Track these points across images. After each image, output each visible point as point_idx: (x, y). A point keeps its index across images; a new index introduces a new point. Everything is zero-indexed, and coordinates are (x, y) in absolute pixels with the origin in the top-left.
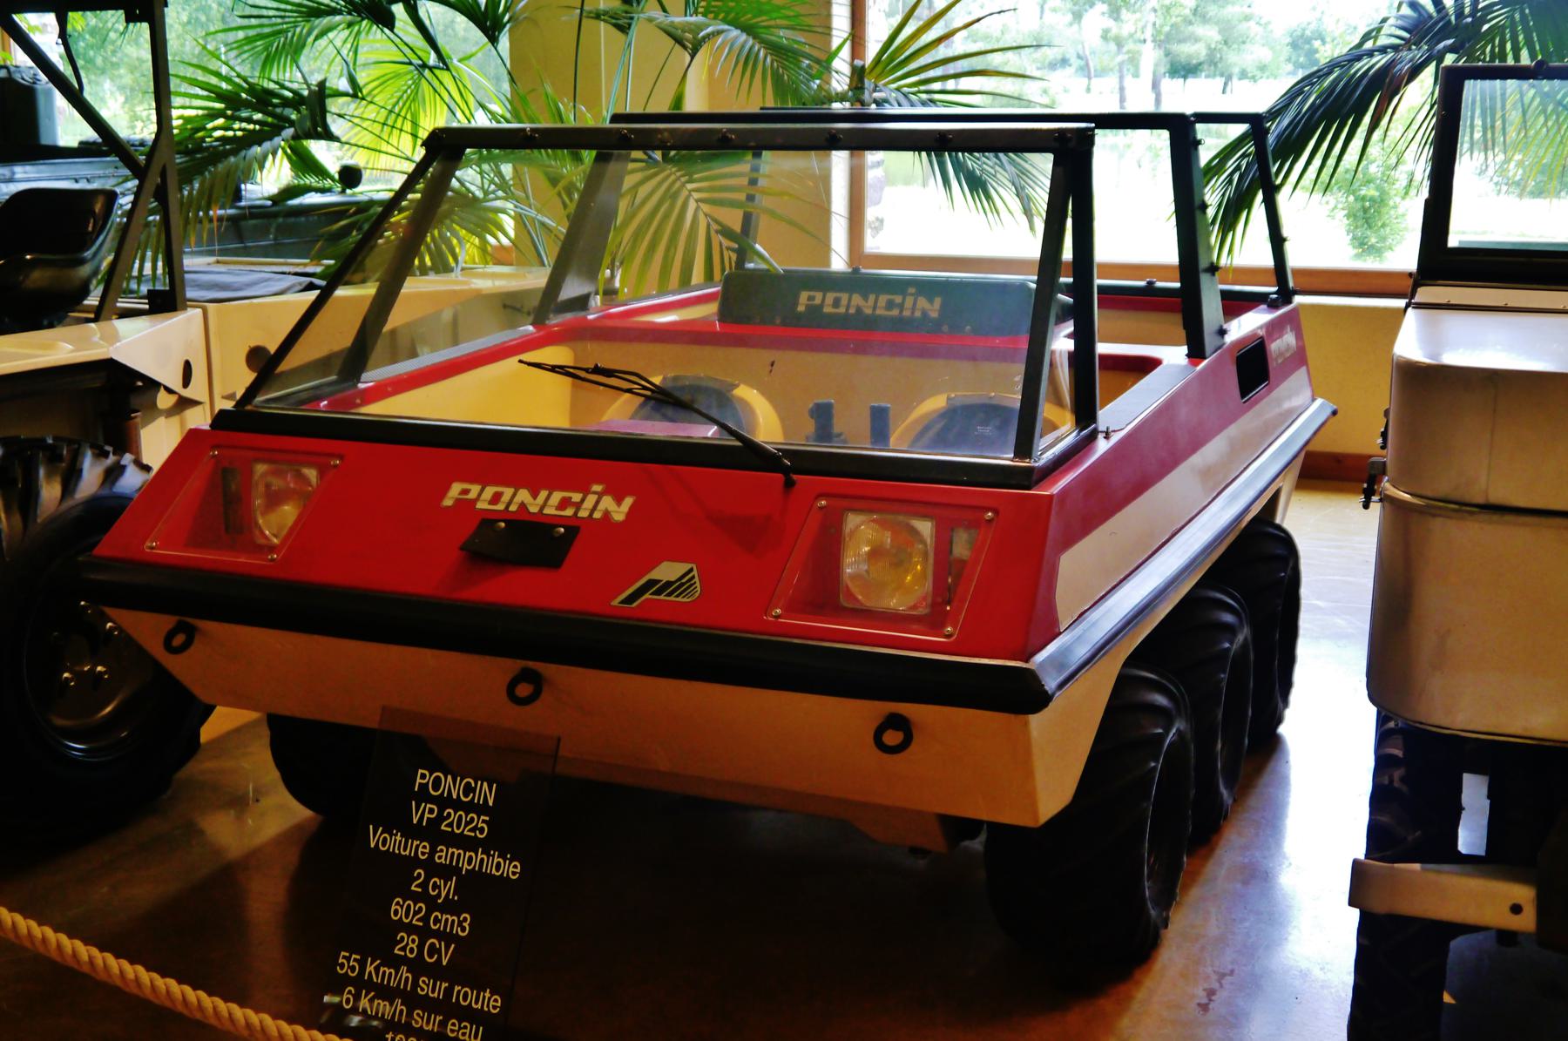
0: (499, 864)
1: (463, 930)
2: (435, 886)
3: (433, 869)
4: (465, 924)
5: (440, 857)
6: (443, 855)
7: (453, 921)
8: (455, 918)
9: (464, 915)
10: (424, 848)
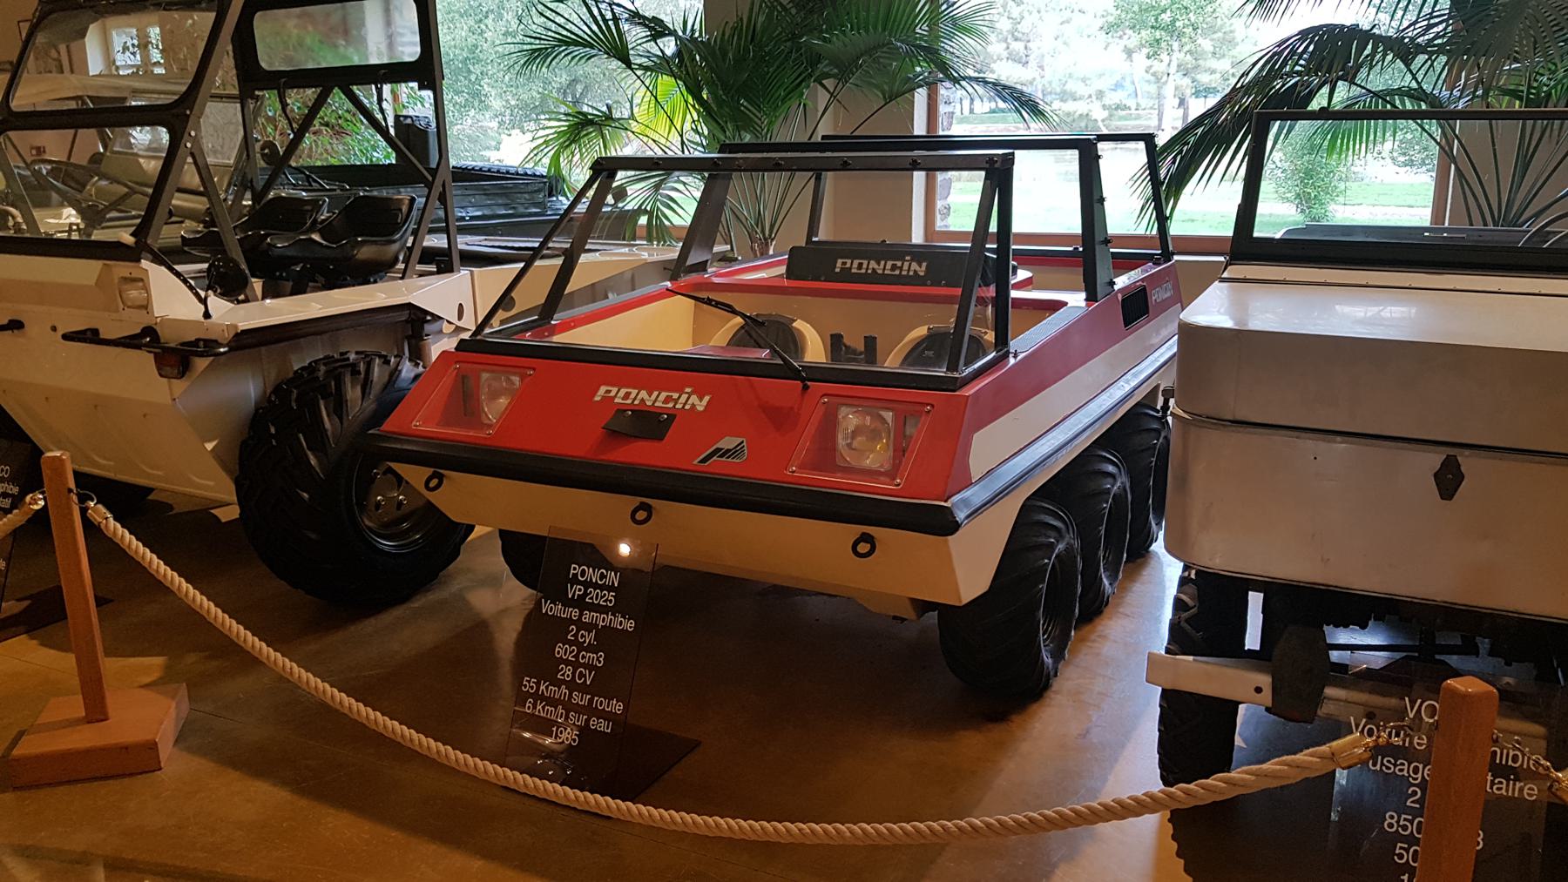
0: (621, 621)
1: (600, 662)
2: (583, 636)
3: (581, 625)
4: (601, 659)
5: (585, 618)
6: (587, 617)
10: (575, 613)
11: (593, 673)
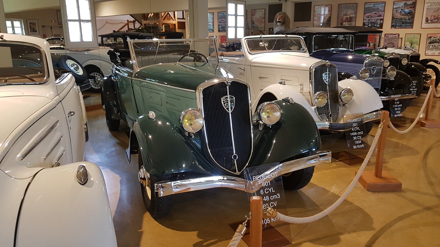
7: (276, 196)
8: (276, 195)
9: (278, 194)
11: (276, 202)
